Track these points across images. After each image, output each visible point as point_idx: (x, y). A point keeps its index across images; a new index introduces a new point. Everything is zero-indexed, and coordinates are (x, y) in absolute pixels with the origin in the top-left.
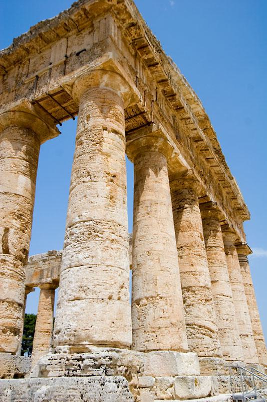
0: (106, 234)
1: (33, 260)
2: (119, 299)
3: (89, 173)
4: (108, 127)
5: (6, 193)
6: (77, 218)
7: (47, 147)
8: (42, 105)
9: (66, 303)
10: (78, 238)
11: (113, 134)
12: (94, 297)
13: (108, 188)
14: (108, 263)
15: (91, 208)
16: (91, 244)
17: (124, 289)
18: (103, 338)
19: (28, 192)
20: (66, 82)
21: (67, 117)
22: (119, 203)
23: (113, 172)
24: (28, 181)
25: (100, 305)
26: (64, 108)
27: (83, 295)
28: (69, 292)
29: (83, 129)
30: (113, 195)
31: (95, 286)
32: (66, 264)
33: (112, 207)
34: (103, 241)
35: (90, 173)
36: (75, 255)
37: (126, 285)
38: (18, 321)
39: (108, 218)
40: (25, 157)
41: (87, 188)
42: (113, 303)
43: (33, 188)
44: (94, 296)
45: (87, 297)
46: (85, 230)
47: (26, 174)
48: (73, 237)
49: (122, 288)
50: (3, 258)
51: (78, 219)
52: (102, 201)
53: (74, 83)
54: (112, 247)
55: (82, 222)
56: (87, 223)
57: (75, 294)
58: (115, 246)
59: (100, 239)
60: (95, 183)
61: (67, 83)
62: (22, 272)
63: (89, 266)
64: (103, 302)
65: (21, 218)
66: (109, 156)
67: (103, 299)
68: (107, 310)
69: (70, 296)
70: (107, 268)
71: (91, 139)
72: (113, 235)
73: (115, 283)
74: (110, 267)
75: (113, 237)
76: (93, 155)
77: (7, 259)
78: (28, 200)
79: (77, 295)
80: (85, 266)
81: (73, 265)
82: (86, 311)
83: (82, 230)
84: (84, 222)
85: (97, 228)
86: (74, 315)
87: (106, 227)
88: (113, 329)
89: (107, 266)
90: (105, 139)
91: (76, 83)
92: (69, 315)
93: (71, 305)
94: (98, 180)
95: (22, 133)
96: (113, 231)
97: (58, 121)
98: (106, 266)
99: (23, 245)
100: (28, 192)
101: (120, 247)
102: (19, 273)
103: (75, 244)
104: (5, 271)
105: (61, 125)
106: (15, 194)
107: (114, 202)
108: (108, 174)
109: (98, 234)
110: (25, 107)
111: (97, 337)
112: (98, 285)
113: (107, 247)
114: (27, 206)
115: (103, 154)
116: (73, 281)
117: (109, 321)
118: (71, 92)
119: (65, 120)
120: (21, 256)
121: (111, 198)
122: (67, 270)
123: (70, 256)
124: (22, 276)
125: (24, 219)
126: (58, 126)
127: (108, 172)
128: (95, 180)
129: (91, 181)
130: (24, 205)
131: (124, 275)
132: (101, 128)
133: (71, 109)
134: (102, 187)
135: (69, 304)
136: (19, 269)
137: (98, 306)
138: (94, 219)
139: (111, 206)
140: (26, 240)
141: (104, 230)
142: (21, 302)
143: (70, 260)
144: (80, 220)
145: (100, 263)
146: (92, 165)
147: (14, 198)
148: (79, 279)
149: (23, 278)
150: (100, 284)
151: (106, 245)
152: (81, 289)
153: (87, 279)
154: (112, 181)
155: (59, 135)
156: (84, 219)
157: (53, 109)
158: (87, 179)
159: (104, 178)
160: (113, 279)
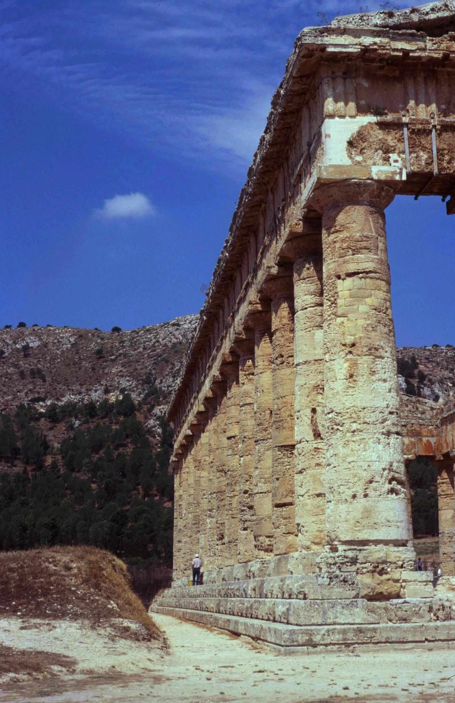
0: (347, 426)
2: (366, 496)
4: (341, 274)
5: (306, 362)
11: (349, 280)
14: (350, 459)
17: (374, 485)
18: (348, 538)
22: (361, 380)
23: (349, 340)
37: (377, 478)
49: (371, 482)
50: (315, 446)
54: (354, 439)
70: (350, 466)
74: (352, 463)
75: (355, 426)
77: (319, 447)
88: (357, 529)
89: (349, 463)
104: (320, 461)
106: (315, 360)
107: (355, 381)
108: (344, 345)
111: (343, 538)
113: (348, 441)
121: (351, 376)
127: (343, 343)
131: (372, 468)
137: (343, 507)
141: (343, 421)
147: (313, 367)
154: (350, 352)
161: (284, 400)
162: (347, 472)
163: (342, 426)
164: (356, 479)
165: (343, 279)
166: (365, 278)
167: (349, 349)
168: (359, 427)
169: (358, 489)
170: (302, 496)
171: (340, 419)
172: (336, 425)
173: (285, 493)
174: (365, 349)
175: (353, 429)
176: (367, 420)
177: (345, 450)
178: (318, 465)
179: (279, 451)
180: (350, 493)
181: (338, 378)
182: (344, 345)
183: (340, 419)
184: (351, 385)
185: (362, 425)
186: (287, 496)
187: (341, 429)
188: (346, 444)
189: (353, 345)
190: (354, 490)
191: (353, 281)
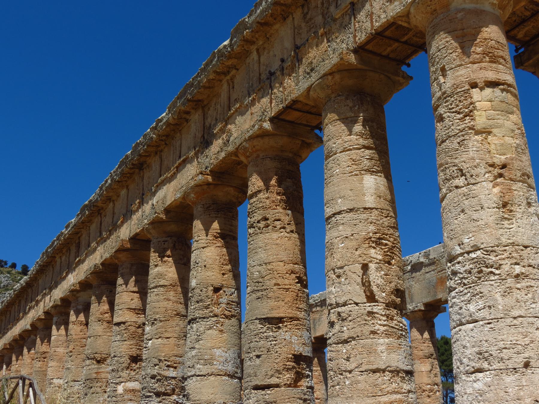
0: (506, 268)
1: (431, 257)
3: (461, 170)
4: (478, 81)
5: (351, 210)
6: (457, 248)
7: (393, 109)
8: (371, 49)
9: (464, 377)
10: (464, 280)
11: (488, 91)
12: (502, 368)
13: (496, 190)
14: (515, 313)
15: (474, 229)
16: (484, 287)
19: (382, 199)
20: (397, 13)
21: (414, 52)
22: (519, 211)
23: (500, 159)
24: (378, 181)
25: (512, 378)
26: (405, 43)
27: (485, 365)
28: (465, 361)
29: (439, 94)
30: (506, 200)
31: (501, 350)
32: (455, 319)
33: (509, 219)
34: (503, 280)
35: (464, 172)
36: (464, 307)
38: (411, 395)
39: (504, 240)
40: (365, 142)
41: (464, 198)
42: (533, 373)
43: (391, 188)
44: (501, 365)
45: (490, 368)
46: (471, 266)
47: (373, 172)
48: (456, 279)
50: (369, 309)
51: (458, 250)
52: (489, 216)
53: (409, 11)
54: (519, 286)
55: (466, 255)
56: (473, 255)
57: (474, 364)
58: (524, 284)
59: (497, 277)
60: (474, 187)
61: (399, 15)
62: (401, 325)
63: (487, 321)
64: (516, 372)
65: (382, 244)
66: (489, 133)
67: (515, 369)
68: (525, 384)
69: (468, 368)
70: (515, 322)
71: (454, 110)
72: (518, 266)
73: (532, 342)
74: (520, 319)
75: (518, 269)
76: (462, 138)
77: (375, 311)
78: (384, 211)
79: (477, 366)
80: (481, 323)
81: (463, 321)
82: (492, 388)
83: (467, 267)
84: (468, 253)
85: (490, 261)
86: (477, 395)
87: (503, 257)
89: (515, 318)
90: (477, 104)
91: (412, 10)
92: (470, 394)
93: (471, 379)
94: (478, 180)
95: (351, 105)
96: (515, 261)
97: (403, 61)
98: (512, 319)
99: (393, 285)
100: (382, 199)
101: (533, 283)
102: (396, 327)
103: (462, 289)
104: (376, 328)
105: (409, 65)
106: (365, 208)
107: (511, 211)
109: (493, 270)
110: (346, 64)
112: (505, 348)
113: (510, 288)
114: (386, 222)
115: (478, 133)
116: (468, 345)
117: (530, 399)
118: (409, 23)
119: (414, 57)
120: (393, 301)
121: (505, 205)
122: (457, 329)
123: (457, 308)
124: (401, 330)
125: (386, 245)
126: (404, 68)
127: (490, 162)
128: (473, 181)
129: (468, 184)
130: (381, 221)
132: (467, 87)
133: (418, 39)
134: (488, 191)
135: (468, 379)
136: (395, 322)
137: (509, 379)
138: (482, 246)
139: (506, 218)
140: (396, 276)
141: (501, 262)
142: (409, 368)
143: (459, 314)
144: (462, 251)
145: (502, 315)
146: (464, 157)
147: (364, 216)
148: (475, 342)
149: (404, 334)
150: (507, 346)
151: (507, 285)
152: (481, 357)
153: (486, 341)
154: (501, 175)
155: (411, 82)
156: (467, 249)
157: (389, 49)
158: (460, 182)
159: (487, 175)
160: (526, 336)
161: (269, 267)
162: (512, 330)
163: (497, 269)
164: (527, 340)
165: (482, 89)
166: (508, 91)
167: (496, 171)
168: (523, 271)
169: (532, 354)
170: (350, 372)
171: (494, 259)
172: (487, 267)
173: (270, 373)
174: (519, 174)
175: (516, 272)
176: (533, 262)
177: (506, 299)
178: (373, 332)
179: (262, 324)
180: (520, 360)
181: (486, 205)
182: (492, 165)
183: (494, 259)
184: (506, 216)
185: (527, 268)
186: (272, 376)
187: (497, 272)
188: (507, 293)
189: (504, 166)
190: (526, 355)
191: (493, 92)
